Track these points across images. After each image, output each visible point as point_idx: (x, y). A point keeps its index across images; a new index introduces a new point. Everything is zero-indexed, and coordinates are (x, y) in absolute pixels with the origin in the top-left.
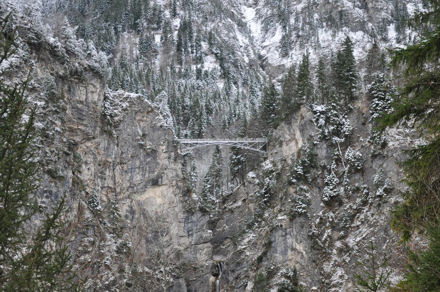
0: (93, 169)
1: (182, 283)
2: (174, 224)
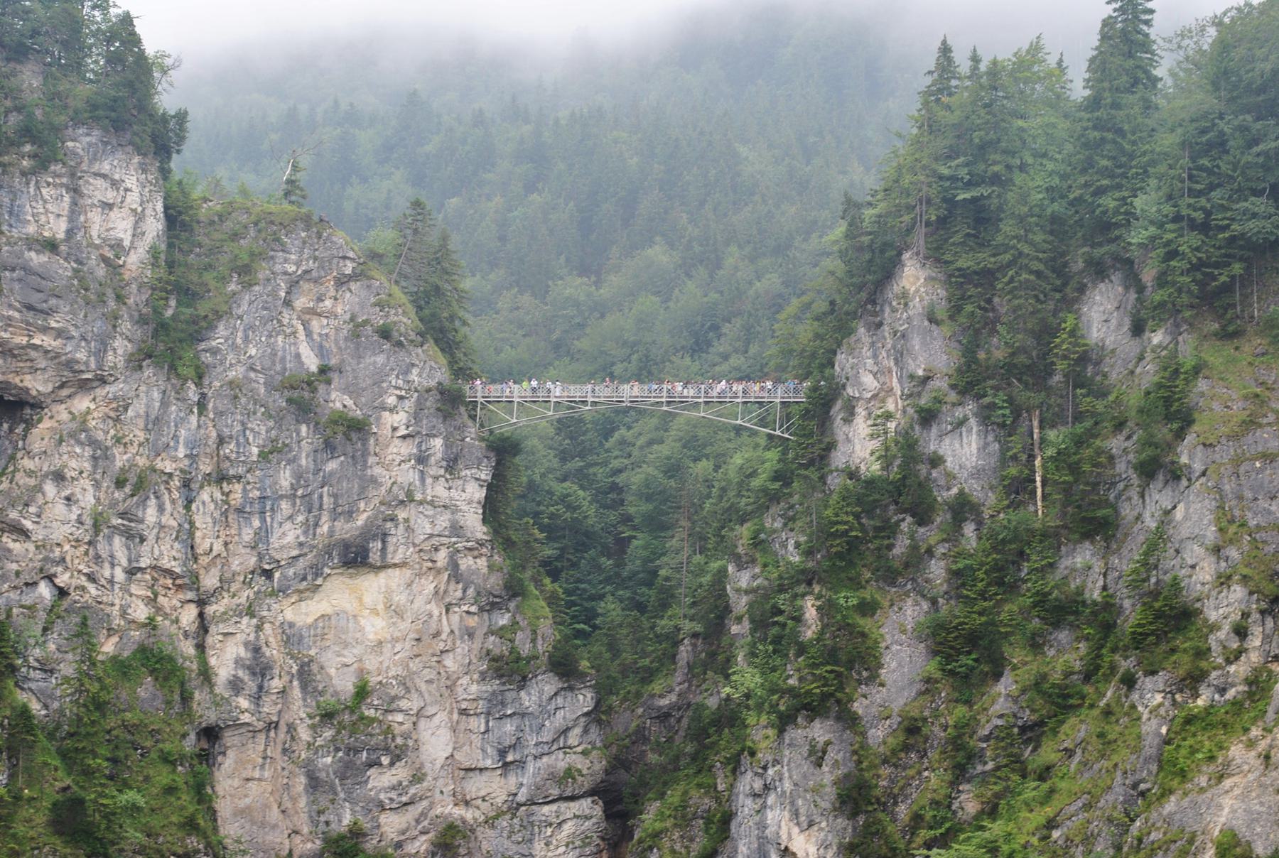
0: (88, 500)
2: (436, 720)
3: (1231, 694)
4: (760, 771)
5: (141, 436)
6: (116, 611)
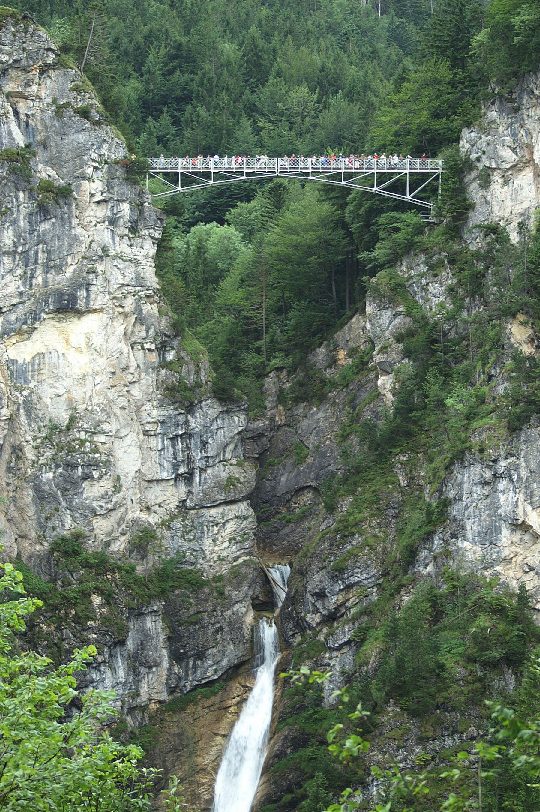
1: (153, 632)
2: (128, 440)
4: (491, 463)
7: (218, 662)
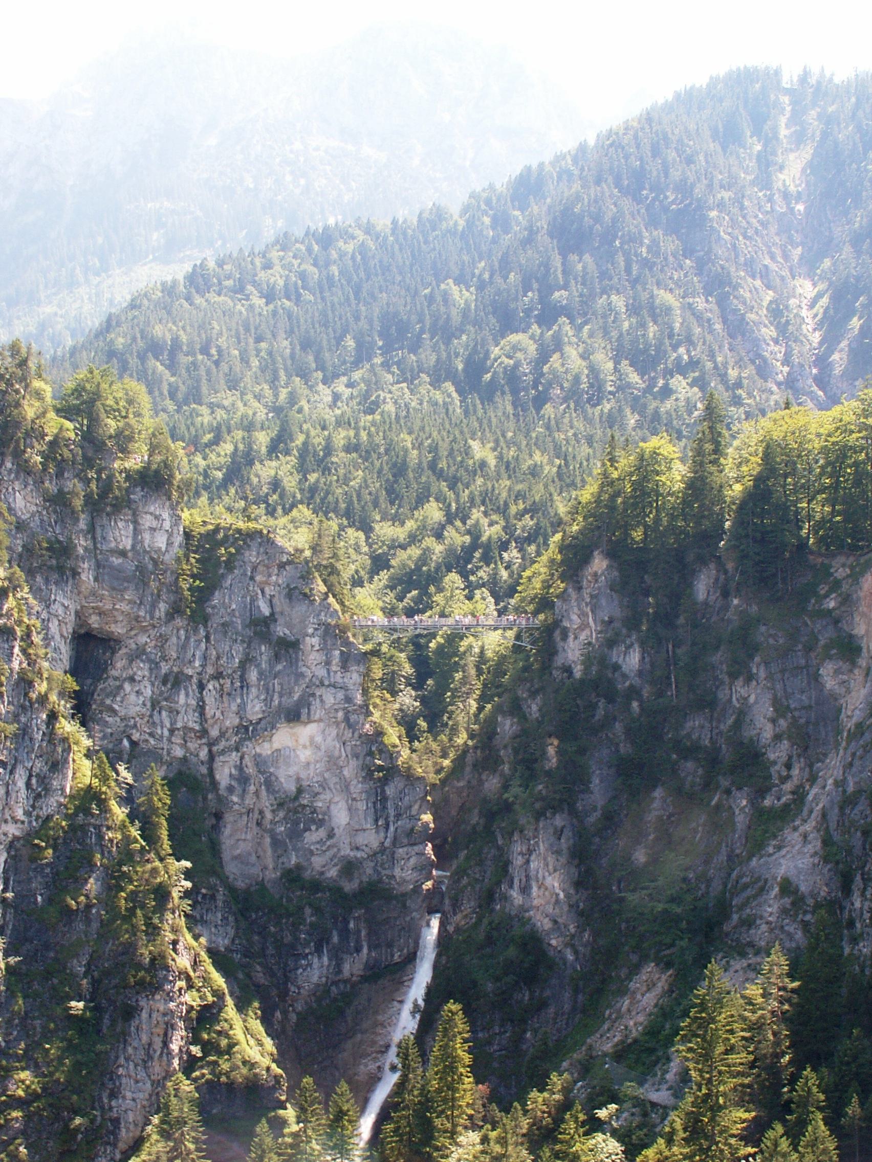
0: (148, 692)
3: (784, 799)
5: (175, 655)
6: (165, 752)
7: (401, 950)
